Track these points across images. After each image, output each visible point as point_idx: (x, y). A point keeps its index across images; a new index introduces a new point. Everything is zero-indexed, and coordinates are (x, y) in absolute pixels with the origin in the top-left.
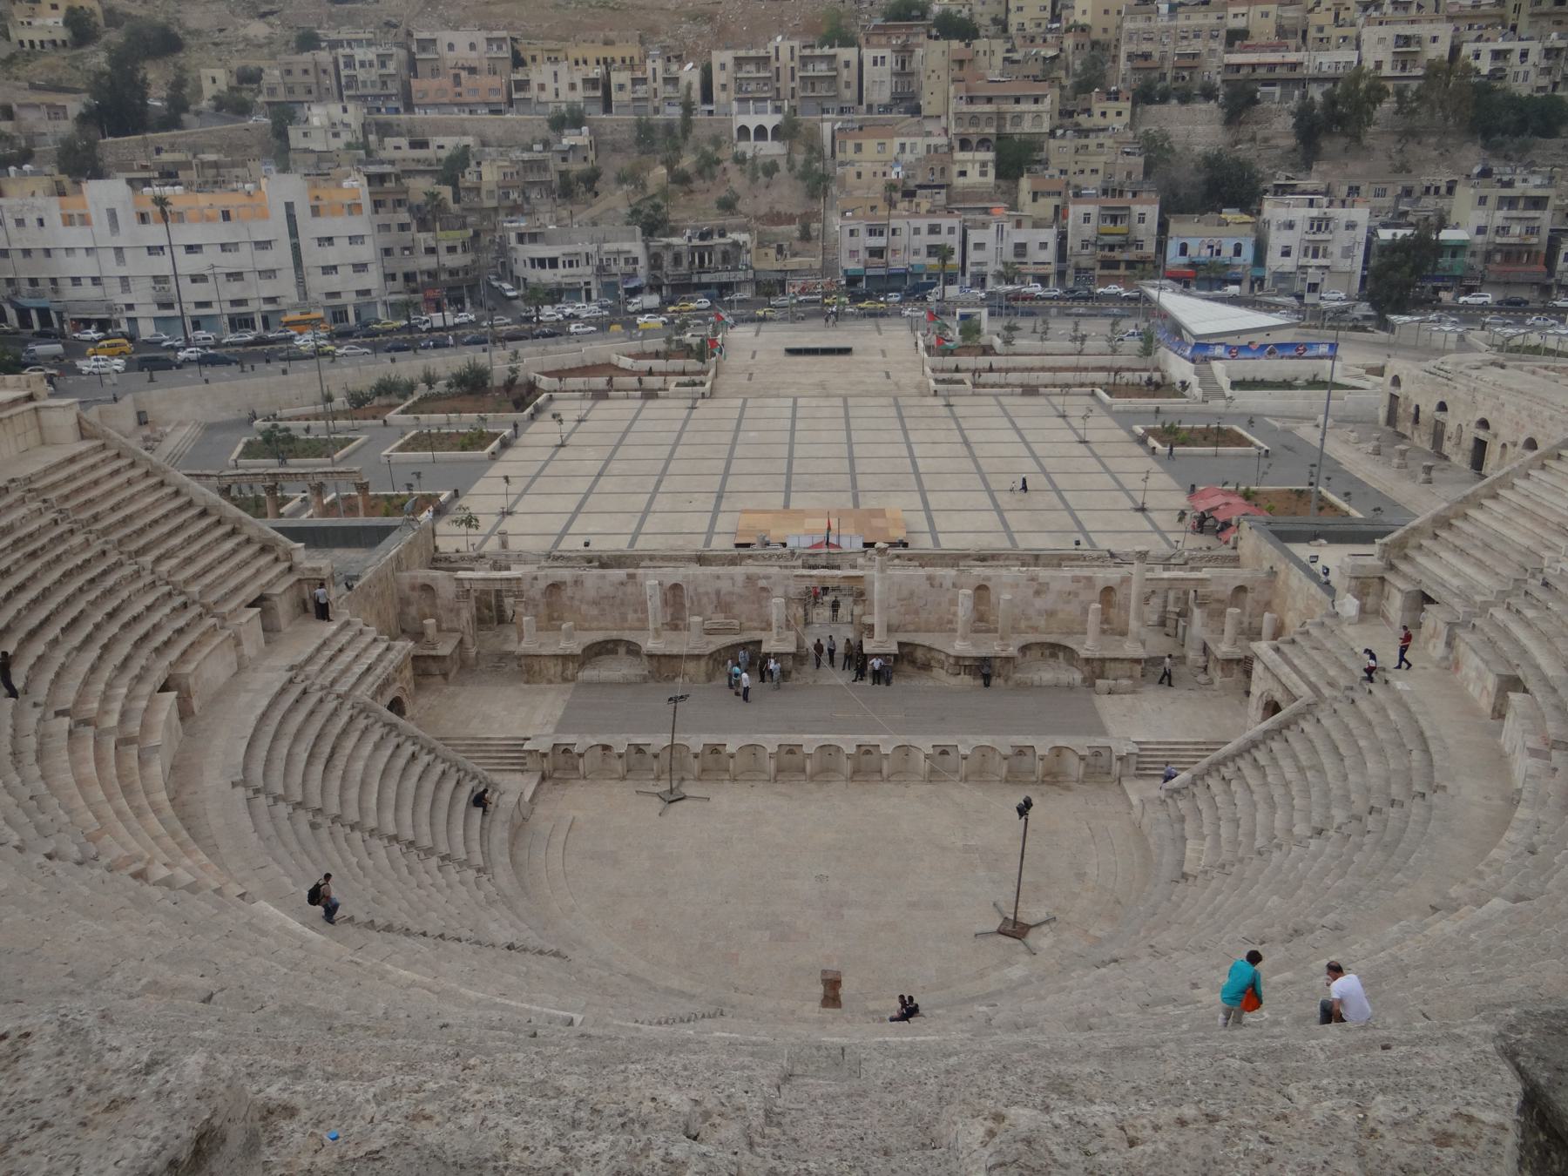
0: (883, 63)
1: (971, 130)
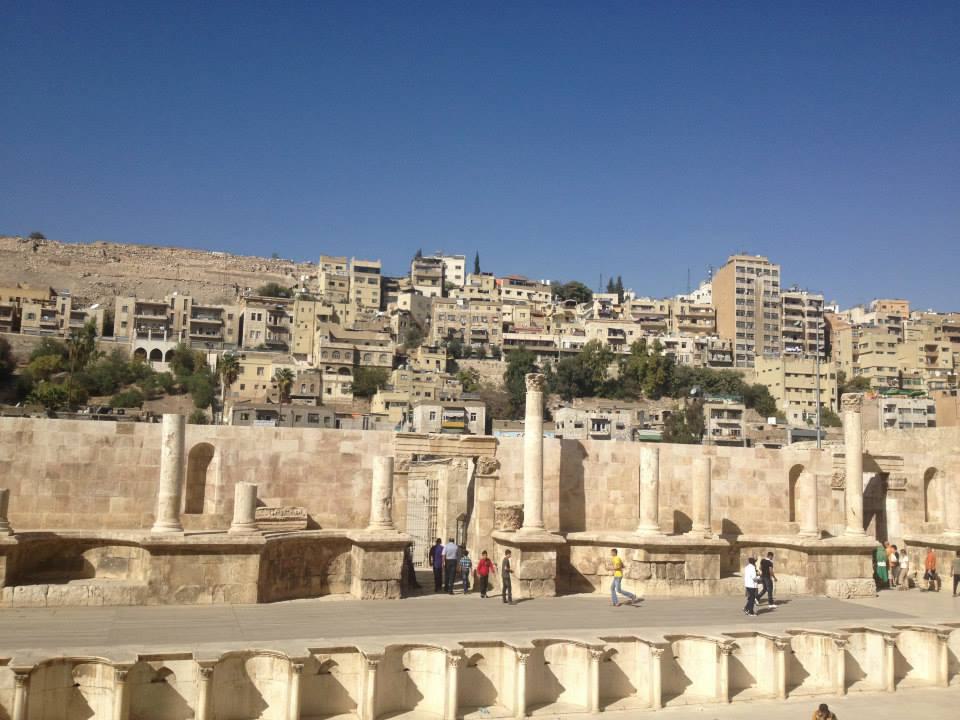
0: (259, 319)
1: (334, 361)
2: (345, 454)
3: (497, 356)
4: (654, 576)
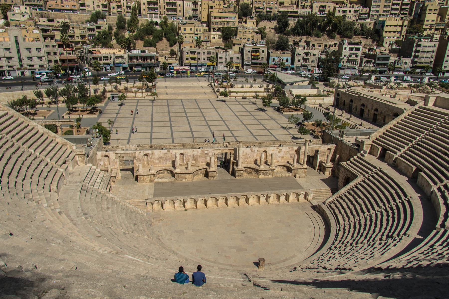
0: (190, 6)
1: (216, 26)
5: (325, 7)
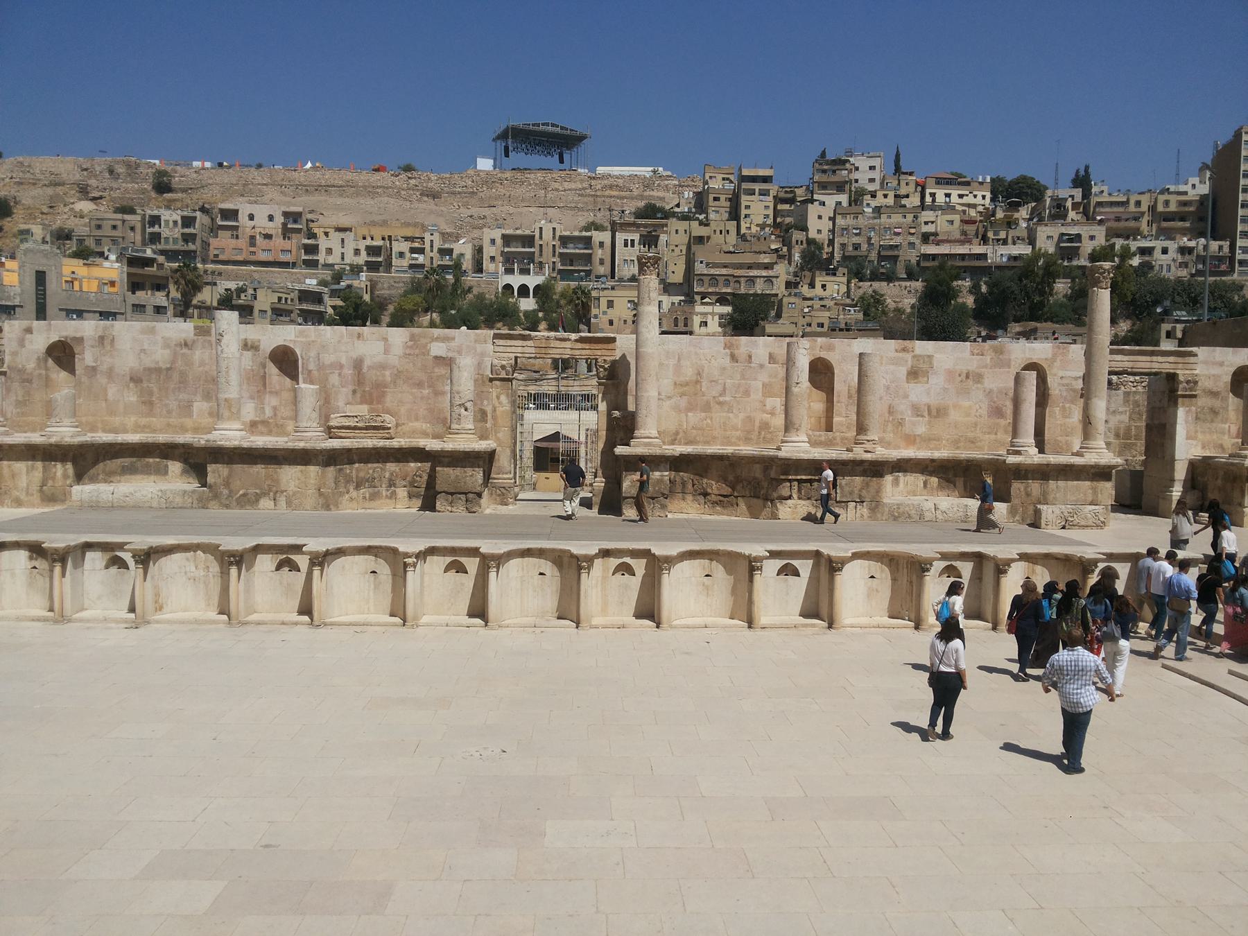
0: (633, 246)
2: (436, 357)
3: (911, 276)
4: (795, 496)
5: (1078, 237)
